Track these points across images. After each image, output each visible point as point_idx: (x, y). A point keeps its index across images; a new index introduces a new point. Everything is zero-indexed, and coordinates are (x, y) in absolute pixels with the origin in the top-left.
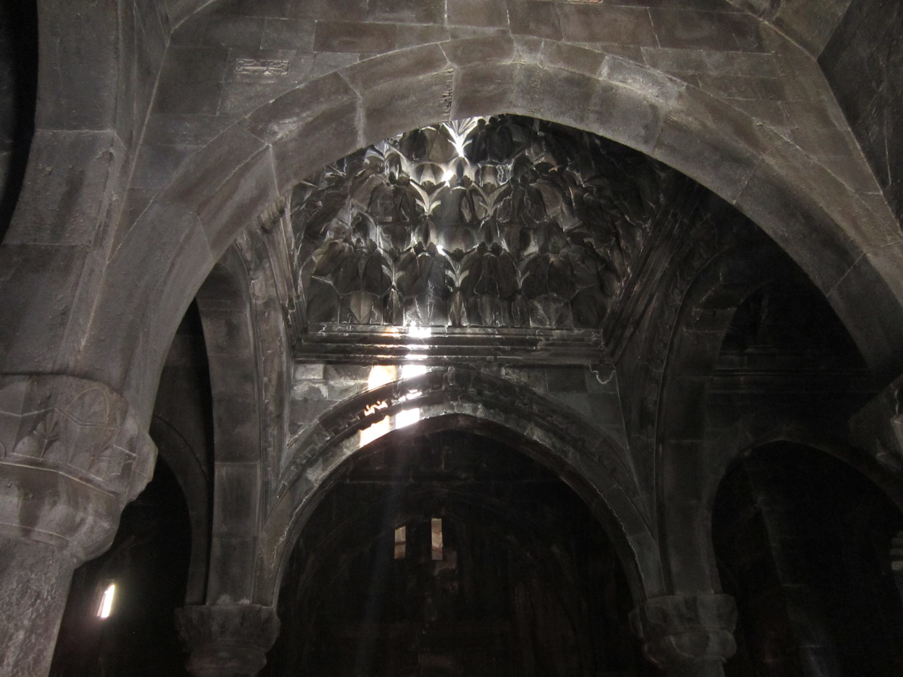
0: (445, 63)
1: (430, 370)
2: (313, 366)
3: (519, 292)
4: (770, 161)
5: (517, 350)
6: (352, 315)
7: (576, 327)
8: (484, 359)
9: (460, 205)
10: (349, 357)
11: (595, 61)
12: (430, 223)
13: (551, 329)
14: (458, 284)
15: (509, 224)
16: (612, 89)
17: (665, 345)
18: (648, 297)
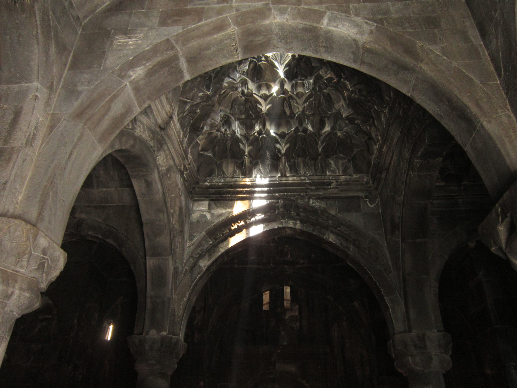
0: (230, 26)
1: (269, 202)
2: (203, 202)
3: (320, 155)
4: (424, 67)
5: (319, 189)
6: (224, 173)
7: (354, 173)
8: (300, 195)
9: (283, 106)
10: (222, 197)
11: (320, 15)
13: (340, 176)
14: (283, 152)
15: (313, 115)
16: (330, 32)
17: (403, 182)
18: (391, 154)
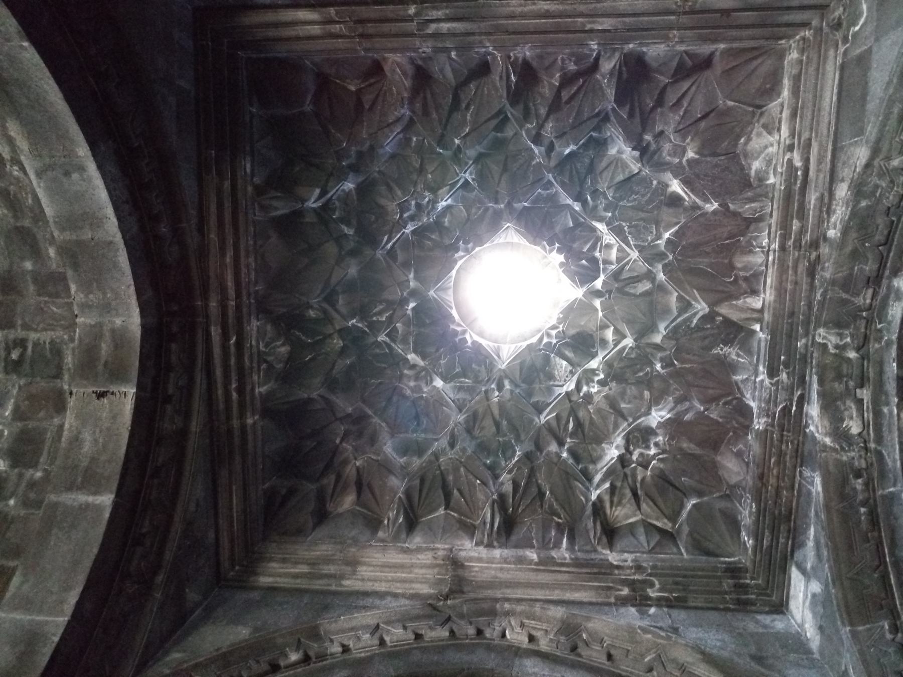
12: (645, 340)
